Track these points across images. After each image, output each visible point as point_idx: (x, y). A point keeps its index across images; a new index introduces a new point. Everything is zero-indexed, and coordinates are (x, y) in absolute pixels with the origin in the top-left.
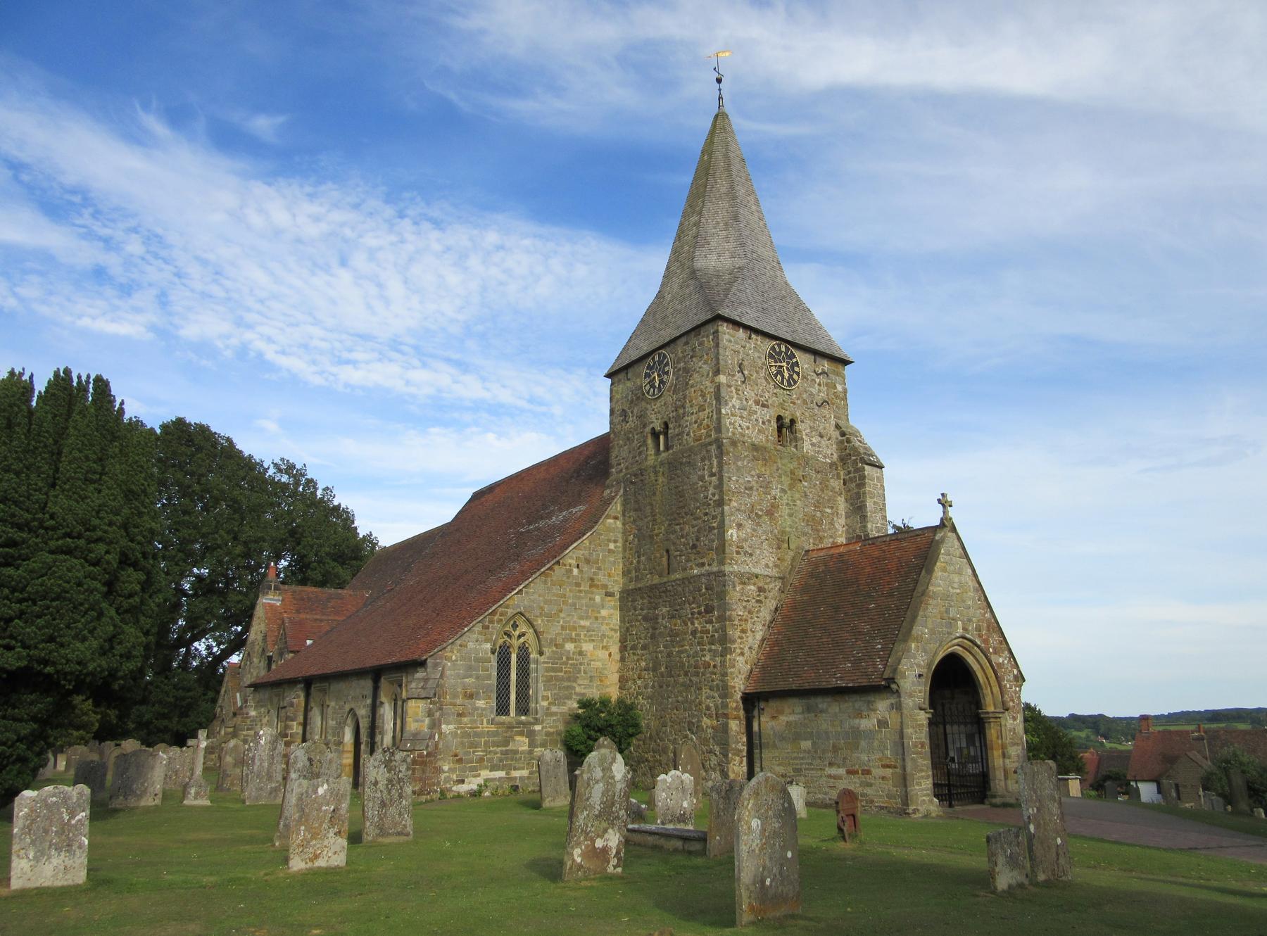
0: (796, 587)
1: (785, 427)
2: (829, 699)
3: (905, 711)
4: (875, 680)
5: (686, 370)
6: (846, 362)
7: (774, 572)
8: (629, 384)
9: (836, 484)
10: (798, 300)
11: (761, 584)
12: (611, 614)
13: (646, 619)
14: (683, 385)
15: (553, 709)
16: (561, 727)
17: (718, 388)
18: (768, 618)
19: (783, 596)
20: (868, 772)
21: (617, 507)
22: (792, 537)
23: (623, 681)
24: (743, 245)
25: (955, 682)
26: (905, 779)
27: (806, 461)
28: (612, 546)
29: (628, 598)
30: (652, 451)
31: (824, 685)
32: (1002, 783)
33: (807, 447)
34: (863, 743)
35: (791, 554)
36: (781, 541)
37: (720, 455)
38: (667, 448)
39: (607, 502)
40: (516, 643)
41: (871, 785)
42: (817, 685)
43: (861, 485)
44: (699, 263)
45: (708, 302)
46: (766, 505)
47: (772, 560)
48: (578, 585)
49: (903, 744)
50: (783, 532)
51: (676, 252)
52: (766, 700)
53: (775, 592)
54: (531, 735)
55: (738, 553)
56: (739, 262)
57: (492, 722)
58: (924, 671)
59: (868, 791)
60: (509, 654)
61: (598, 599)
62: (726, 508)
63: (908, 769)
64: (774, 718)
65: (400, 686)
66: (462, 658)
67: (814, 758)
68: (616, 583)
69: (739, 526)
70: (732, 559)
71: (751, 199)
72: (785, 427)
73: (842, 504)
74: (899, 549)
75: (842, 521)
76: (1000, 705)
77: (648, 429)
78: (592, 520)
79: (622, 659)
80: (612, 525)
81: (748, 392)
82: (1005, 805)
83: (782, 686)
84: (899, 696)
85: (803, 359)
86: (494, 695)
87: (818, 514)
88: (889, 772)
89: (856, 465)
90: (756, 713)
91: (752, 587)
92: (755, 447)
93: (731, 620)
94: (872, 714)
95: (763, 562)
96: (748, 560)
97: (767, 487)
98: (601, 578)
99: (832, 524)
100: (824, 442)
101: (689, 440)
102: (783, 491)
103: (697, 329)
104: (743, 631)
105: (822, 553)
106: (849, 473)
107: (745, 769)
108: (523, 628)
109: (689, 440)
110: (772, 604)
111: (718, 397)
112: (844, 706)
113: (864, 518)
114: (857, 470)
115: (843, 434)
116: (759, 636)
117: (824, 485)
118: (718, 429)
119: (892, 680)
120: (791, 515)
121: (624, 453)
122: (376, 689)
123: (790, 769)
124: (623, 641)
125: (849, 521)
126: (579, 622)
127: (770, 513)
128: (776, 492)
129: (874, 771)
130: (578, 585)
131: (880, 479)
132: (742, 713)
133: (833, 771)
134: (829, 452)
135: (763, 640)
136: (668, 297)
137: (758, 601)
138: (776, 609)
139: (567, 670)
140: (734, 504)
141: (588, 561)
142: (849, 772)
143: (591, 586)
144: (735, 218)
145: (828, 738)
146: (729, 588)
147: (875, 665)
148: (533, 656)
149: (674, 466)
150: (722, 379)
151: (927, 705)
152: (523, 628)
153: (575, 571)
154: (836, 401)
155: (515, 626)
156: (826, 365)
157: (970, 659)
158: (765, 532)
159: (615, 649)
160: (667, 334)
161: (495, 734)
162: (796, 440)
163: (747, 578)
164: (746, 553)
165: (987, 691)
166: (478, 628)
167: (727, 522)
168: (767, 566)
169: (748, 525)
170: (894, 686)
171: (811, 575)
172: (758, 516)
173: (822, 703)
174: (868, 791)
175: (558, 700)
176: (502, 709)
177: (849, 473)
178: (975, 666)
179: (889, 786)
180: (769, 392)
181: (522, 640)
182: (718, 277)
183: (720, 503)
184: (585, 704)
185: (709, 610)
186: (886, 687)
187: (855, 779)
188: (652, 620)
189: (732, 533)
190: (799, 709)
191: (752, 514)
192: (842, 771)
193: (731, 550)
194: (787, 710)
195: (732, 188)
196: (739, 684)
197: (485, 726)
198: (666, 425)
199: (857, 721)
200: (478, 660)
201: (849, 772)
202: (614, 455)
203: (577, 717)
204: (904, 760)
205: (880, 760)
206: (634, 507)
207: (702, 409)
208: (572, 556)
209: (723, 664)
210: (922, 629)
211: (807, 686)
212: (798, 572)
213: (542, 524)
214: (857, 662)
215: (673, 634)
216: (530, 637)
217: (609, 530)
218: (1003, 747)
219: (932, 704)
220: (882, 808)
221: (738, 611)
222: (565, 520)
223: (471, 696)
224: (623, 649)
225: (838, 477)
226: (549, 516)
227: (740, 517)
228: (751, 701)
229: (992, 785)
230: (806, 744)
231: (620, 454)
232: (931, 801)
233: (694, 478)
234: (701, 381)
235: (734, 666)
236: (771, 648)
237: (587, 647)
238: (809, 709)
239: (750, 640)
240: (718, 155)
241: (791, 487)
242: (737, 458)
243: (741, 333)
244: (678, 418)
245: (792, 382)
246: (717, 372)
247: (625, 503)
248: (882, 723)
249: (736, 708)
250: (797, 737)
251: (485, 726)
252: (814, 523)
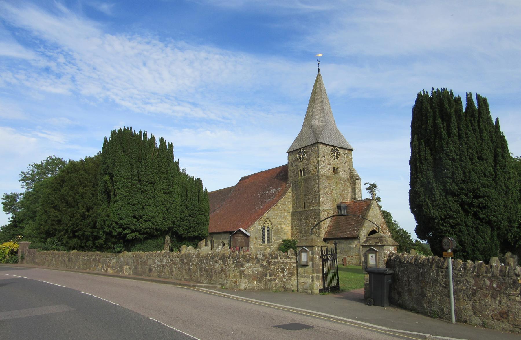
1: (335, 170)
5: (310, 155)
6: (352, 150)
7: (331, 208)
8: (293, 156)
9: (349, 184)
10: (340, 133)
12: (289, 218)
13: (299, 219)
14: (308, 159)
15: (276, 242)
16: (278, 246)
17: (318, 161)
21: (290, 190)
23: (292, 235)
24: (325, 118)
27: (340, 179)
29: (293, 214)
30: (300, 175)
33: (341, 175)
36: (334, 200)
37: (319, 179)
38: (304, 175)
39: (288, 188)
40: (267, 226)
43: (355, 185)
44: (313, 124)
45: (316, 138)
46: (330, 191)
47: (331, 205)
51: (306, 118)
54: (270, 248)
56: (324, 124)
68: (290, 210)
69: (323, 197)
71: (327, 102)
72: (335, 170)
73: (350, 190)
75: (350, 194)
77: (299, 169)
78: (284, 193)
79: (292, 229)
80: (289, 194)
81: (326, 162)
83: (333, 237)
85: (340, 150)
89: (354, 179)
92: (327, 177)
97: (330, 186)
98: (287, 209)
100: (346, 173)
101: (310, 174)
103: (313, 145)
108: (268, 222)
109: (310, 174)
111: (318, 164)
113: (355, 194)
114: (354, 181)
115: (351, 171)
116: (328, 225)
117: (345, 185)
118: (318, 172)
121: (292, 175)
124: (292, 225)
126: (281, 219)
127: (331, 193)
128: (332, 188)
131: (360, 183)
134: (347, 176)
136: (304, 132)
139: (278, 233)
141: (283, 204)
144: (323, 110)
148: (271, 229)
149: (306, 180)
150: (319, 159)
152: (268, 222)
154: (349, 161)
156: (347, 151)
159: (290, 227)
160: (305, 144)
161: (262, 248)
162: (338, 173)
166: (258, 222)
169: (325, 197)
175: (277, 240)
176: (264, 242)
180: (331, 161)
182: (318, 129)
183: (319, 191)
184: (284, 241)
185: (315, 218)
188: (300, 220)
189: (321, 199)
191: (326, 194)
195: (322, 100)
197: (260, 246)
198: (304, 169)
202: (289, 175)
203: (282, 244)
206: (295, 190)
207: (314, 166)
208: (279, 203)
209: (319, 231)
213: (268, 192)
215: (306, 224)
216: (270, 224)
217: (289, 196)
222: (275, 192)
223: (257, 239)
224: (292, 227)
226: (270, 190)
231: (291, 175)
233: (312, 184)
234: (313, 159)
237: (283, 226)
240: (318, 89)
241: (336, 186)
242: (323, 180)
243: (324, 146)
244: (307, 168)
245: (337, 157)
246: (318, 157)
247: (293, 189)
251: (260, 246)
252: (342, 195)
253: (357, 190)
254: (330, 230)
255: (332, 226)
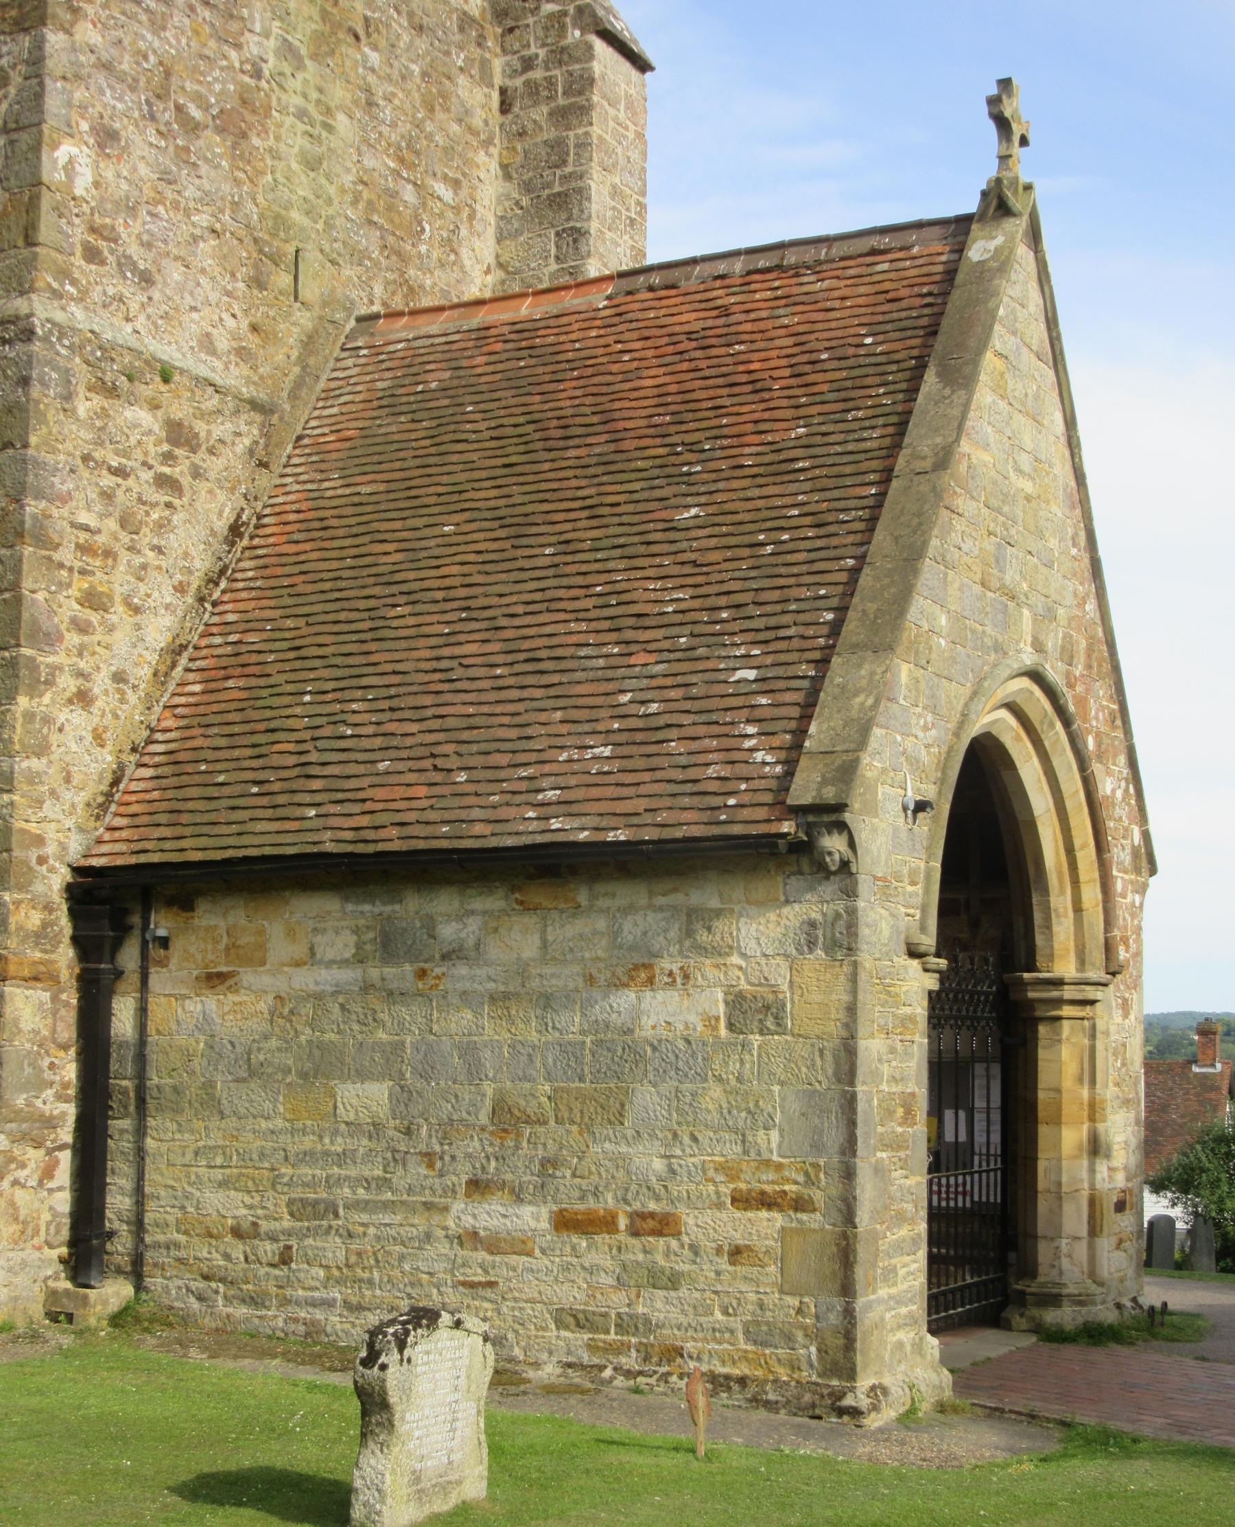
0: (319, 448)
2: (493, 902)
3: (866, 958)
4: (747, 817)
9: (479, 100)
11: (180, 410)
18: (202, 563)
19: (265, 480)
20: (664, 1225)
22: (311, 257)
25: (989, 854)
26: (845, 1255)
31: (481, 834)
32: (1081, 1250)
34: (647, 1099)
35: (305, 319)
36: (267, 257)
41: (674, 1281)
42: (442, 836)
46: (219, 86)
47: (229, 328)
49: (850, 1102)
50: (280, 223)
52: (185, 903)
53: (230, 461)
55: (92, 255)
58: (929, 791)
59: (658, 1306)
62: (54, 39)
63: (863, 1217)
64: (214, 980)
67: (398, 1159)
69: (106, 138)
70: (64, 274)
74: (788, 300)
76: (1098, 956)
82: (1095, 1334)
83: (264, 837)
84: (850, 893)
87: (409, 194)
88: (766, 1226)
90: (129, 957)
91: (143, 416)
93: (44, 541)
94: (708, 970)
95: (195, 323)
96: (135, 301)
99: (450, 245)
102: (287, 50)
104: (93, 600)
105: (434, 326)
106: (528, 64)
107: (63, 1201)
110: (215, 507)
112: (564, 931)
114: (561, 55)
116: (159, 630)
119: (831, 815)
120: (312, 164)
123: (277, 1202)
125: (511, 250)
129: (690, 1220)
131: (637, 109)
132: (65, 957)
133: (490, 1215)
135: (176, 650)
137: (163, 481)
138: (235, 530)
140: (87, 33)
142: (565, 1223)
145: (474, 1073)
146: (45, 396)
147: (732, 753)
151: (929, 941)
157: (1029, 771)
158: (207, 199)
163: (122, 375)
164: (125, 264)
165: (1060, 900)
167: (53, 103)
168: (207, 344)
169: (144, 151)
170: (834, 844)
171: (389, 404)
172: (194, 128)
173: (454, 916)
174: (658, 1306)
177: (528, 64)
178: (1040, 801)
179: (762, 1290)
186: (797, 846)
187: (597, 1253)
189: (70, 161)
190: (340, 944)
192: (532, 1218)
193: (59, 232)
194: (280, 948)
196: (62, 832)
199: (624, 1000)
201: (565, 1223)
204: (849, 1174)
205: (730, 1171)
210: (934, 611)
211: (393, 841)
212: (328, 395)
214: (642, 737)
218: (1094, 1111)
219: (945, 945)
220: (719, 1383)
221: (72, 504)
225: (485, 77)
227: (116, 103)
228: (111, 906)
229: (1044, 1252)
230: (366, 1098)
232: (918, 1347)
235: (42, 750)
236: (213, 679)
238: (389, 945)
239: (121, 639)
241: (323, 48)
248: (752, 1011)
249: (41, 936)
250: (321, 1067)
253: (599, 187)
254: (198, 719)
255: (237, 662)
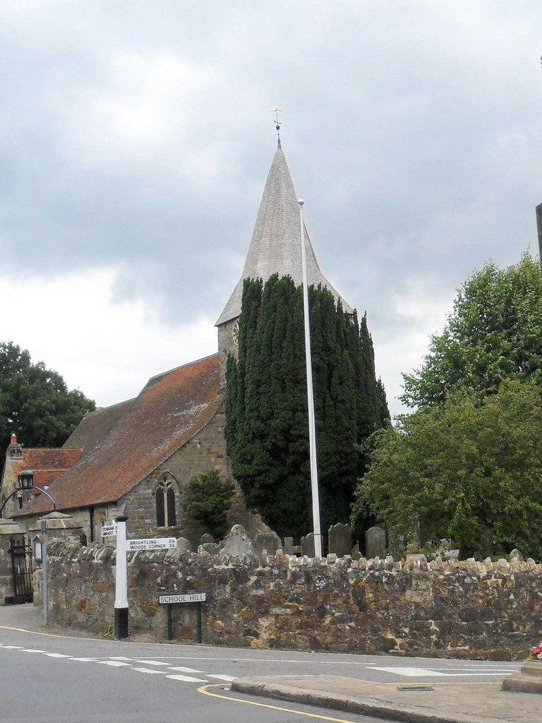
28: (220, 429)
40: (166, 488)
48: (201, 453)
57: (155, 530)
60: (163, 496)
61: (213, 460)
65: (105, 514)
66: (137, 499)
86: (155, 516)
98: (215, 449)
122: (92, 516)
130: (201, 453)
141: (206, 439)
143: (209, 453)
148: (177, 494)
153: (198, 446)
155: (165, 479)
181: (169, 486)
200: (145, 499)
